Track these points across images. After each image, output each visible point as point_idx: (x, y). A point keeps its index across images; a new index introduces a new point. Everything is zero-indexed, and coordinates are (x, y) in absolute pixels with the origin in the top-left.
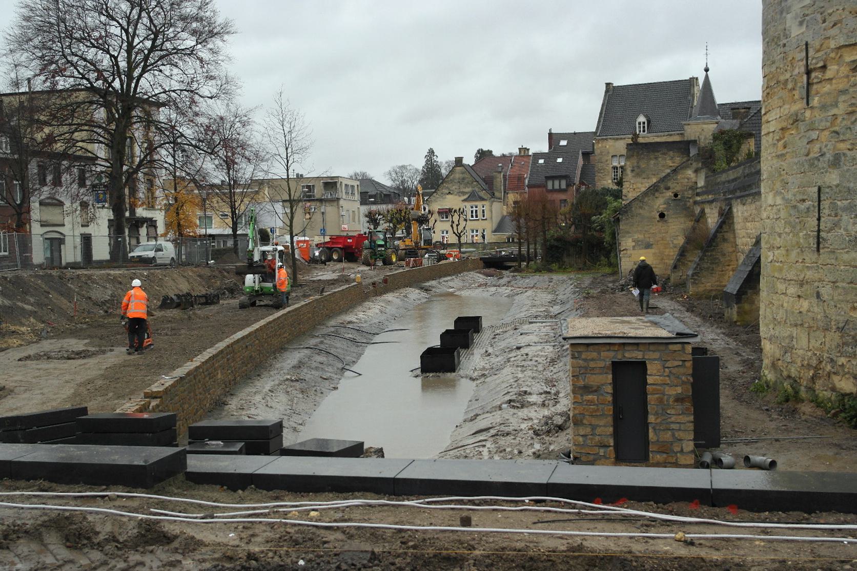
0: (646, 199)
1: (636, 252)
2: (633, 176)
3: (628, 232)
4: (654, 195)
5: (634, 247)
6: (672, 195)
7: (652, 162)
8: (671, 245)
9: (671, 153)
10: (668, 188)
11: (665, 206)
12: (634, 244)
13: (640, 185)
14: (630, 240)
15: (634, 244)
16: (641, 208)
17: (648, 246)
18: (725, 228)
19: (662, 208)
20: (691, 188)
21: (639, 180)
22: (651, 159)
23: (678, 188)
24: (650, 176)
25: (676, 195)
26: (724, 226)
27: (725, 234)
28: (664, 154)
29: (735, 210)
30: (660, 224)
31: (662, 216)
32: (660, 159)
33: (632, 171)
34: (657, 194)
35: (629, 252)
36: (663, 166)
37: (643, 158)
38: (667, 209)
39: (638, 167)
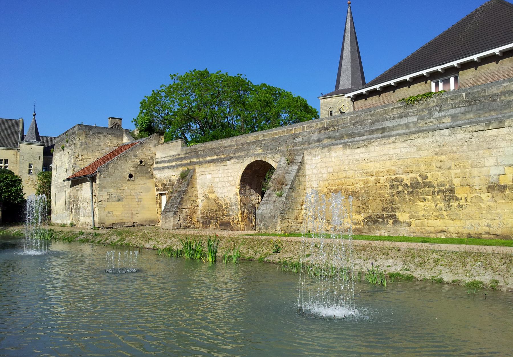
0: (119, 162)
1: (109, 203)
2: (82, 150)
3: (105, 188)
4: (126, 159)
5: (108, 199)
6: (138, 161)
7: (96, 141)
8: (137, 200)
9: (110, 136)
10: (136, 156)
11: (133, 169)
12: (108, 197)
13: (86, 157)
14: (106, 193)
15: (108, 197)
16: (116, 169)
17: (119, 199)
18: (301, 172)
19: (131, 170)
20: (152, 158)
21: (86, 152)
22: (95, 138)
23: (142, 157)
24: (95, 151)
25: (141, 162)
26: (300, 171)
27: (300, 178)
28: (105, 136)
29: (306, 158)
30: (130, 183)
31: (131, 176)
33: (81, 145)
34: (128, 159)
37: (89, 137)
38: (135, 172)
39: (86, 143)
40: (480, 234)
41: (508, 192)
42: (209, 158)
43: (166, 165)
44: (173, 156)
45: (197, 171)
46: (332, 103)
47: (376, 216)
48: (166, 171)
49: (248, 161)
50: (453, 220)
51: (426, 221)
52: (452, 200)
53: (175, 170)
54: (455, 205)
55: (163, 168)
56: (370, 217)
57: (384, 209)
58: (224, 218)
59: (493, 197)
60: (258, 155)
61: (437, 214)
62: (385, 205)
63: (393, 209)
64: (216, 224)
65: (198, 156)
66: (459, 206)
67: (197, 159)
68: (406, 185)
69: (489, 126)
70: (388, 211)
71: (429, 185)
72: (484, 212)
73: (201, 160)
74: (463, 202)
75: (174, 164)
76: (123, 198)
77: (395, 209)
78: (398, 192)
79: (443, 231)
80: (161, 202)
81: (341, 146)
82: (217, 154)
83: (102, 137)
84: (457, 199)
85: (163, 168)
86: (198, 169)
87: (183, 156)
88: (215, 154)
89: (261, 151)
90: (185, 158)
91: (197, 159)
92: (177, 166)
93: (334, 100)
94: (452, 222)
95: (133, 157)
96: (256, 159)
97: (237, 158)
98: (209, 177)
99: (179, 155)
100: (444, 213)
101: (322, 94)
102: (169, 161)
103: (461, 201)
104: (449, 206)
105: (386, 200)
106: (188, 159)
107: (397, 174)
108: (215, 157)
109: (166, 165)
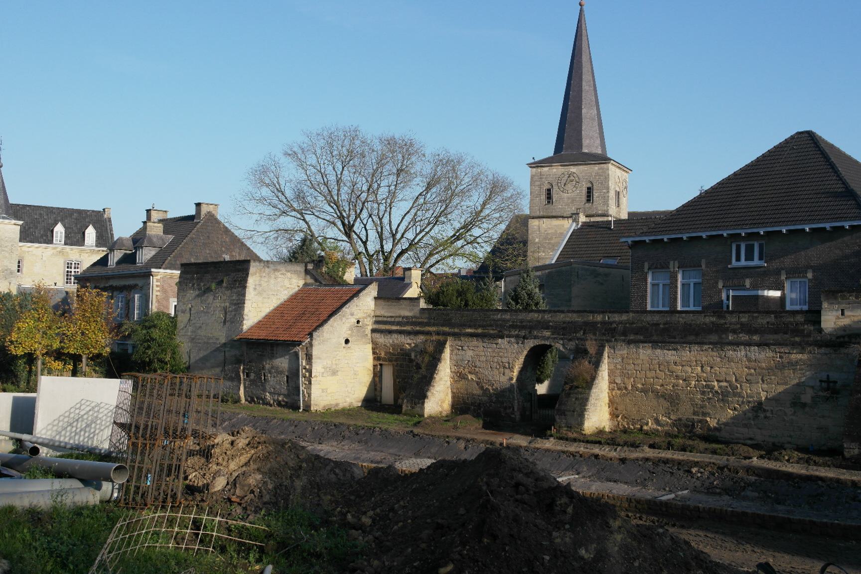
5: (323, 373)
7: (272, 281)
9: (289, 274)
10: (352, 314)
12: (323, 370)
15: (323, 370)
17: (334, 373)
25: (358, 322)
30: (344, 350)
31: (347, 341)
32: (279, 280)
33: (255, 289)
34: (344, 319)
35: (318, 379)
36: (282, 287)
38: (351, 335)
40: (783, 443)
41: (807, 409)
42: (469, 330)
43: (394, 328)
44: (407, 317)
46: (550, 175)
47: (686, 420)
48: (395, 336)
49: (531, 344)
50: (760, 429)
51: (735, 428)
52: (760, 411)
53: (412, 337)
54: (762, 415)
56: (680, 419)
57: (695, 413)
58: (491, 405)
59: (795, 412)
60: (544, 338)
61: (746, 422)
62: (696, 409)
63: (704, 414)
66: (766, 417)
67: (449, 328)
68: (717, 392)
69: (793, 350)
70: (698, 415)
71: (740, 395)
72: (787, 424)
73: (456, 330)
74: (768, 414)
75: (408, 328)
76: (337, 371)
77: (705, 414)
78: (709, 399)
79: (751, 439)
80: (381, 375)
81: (650, 345)
82: (483, 327)
83: (280, 276)
84: (765, 411)
85: (390, 332)
87: (426, 321)
88: (480, 326)
89: (549, 333)
90: (428, 324)
91: (449, 328)
92: (417, 333)
93: (555, 170)
94: (759, 431)
95: (350, 317)
96: (543, 342)
97: (517, 337)
98: (470, 353)
99: (415, 317)
100: (752, 422)
101: (533, 158)
102: (398, 324)
103: (768, 413)
104: (757, 417)
105: (697, 404)
106: (434, 325)
107: (709, 381)
108: (480, 331)
109: (394, 328)
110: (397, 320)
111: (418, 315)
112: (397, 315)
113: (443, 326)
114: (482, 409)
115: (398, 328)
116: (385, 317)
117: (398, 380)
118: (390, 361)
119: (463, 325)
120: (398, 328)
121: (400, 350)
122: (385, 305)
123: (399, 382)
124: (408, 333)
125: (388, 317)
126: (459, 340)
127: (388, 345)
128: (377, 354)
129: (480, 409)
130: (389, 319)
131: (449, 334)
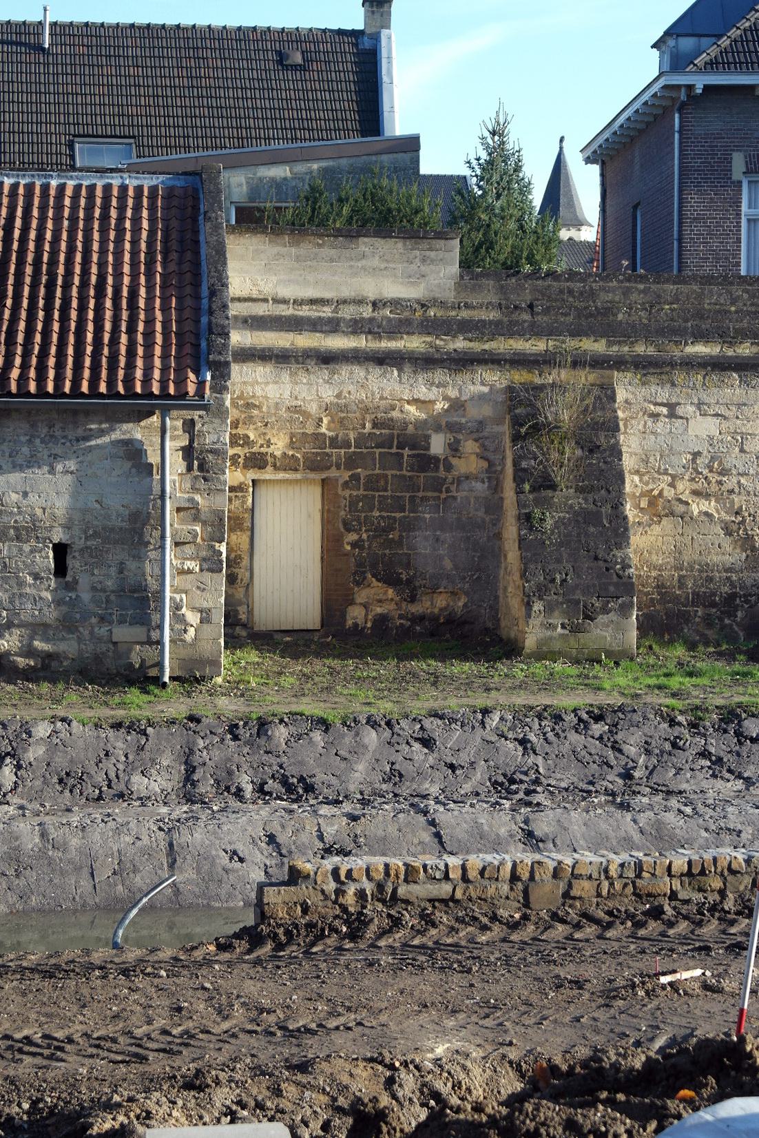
44: (395, 303)
45: (621, 395)
53: (439, 375)
55: (327, 359)
64: (727, 621)
65: (611, 332)
67: (610, 344)
75: (414, 343)
85: (327, 359)
86: (626, 389)
87: (493, 315)
91: (610, 344)
92: (462, 362)
102: (357, 326)
110: (347, 313)
111: (450, 296)
112: (346, 293)
113: (576, 333)
114: (739, 614)
115: (360, 342)
116: (276, 301)
117: (353, 537)
118: (314, 465)
119: (678, 334)
120: (360, 342)
121: (375, 425)
122: (279, 256)
123: (354, 545)
124: (426, 362)
125: (298, 303)
126: (662, 384)
127: (313, 408)
128: (247, 442)
129: (732, 615)
130: (305, 312)
131: (619, 364)
